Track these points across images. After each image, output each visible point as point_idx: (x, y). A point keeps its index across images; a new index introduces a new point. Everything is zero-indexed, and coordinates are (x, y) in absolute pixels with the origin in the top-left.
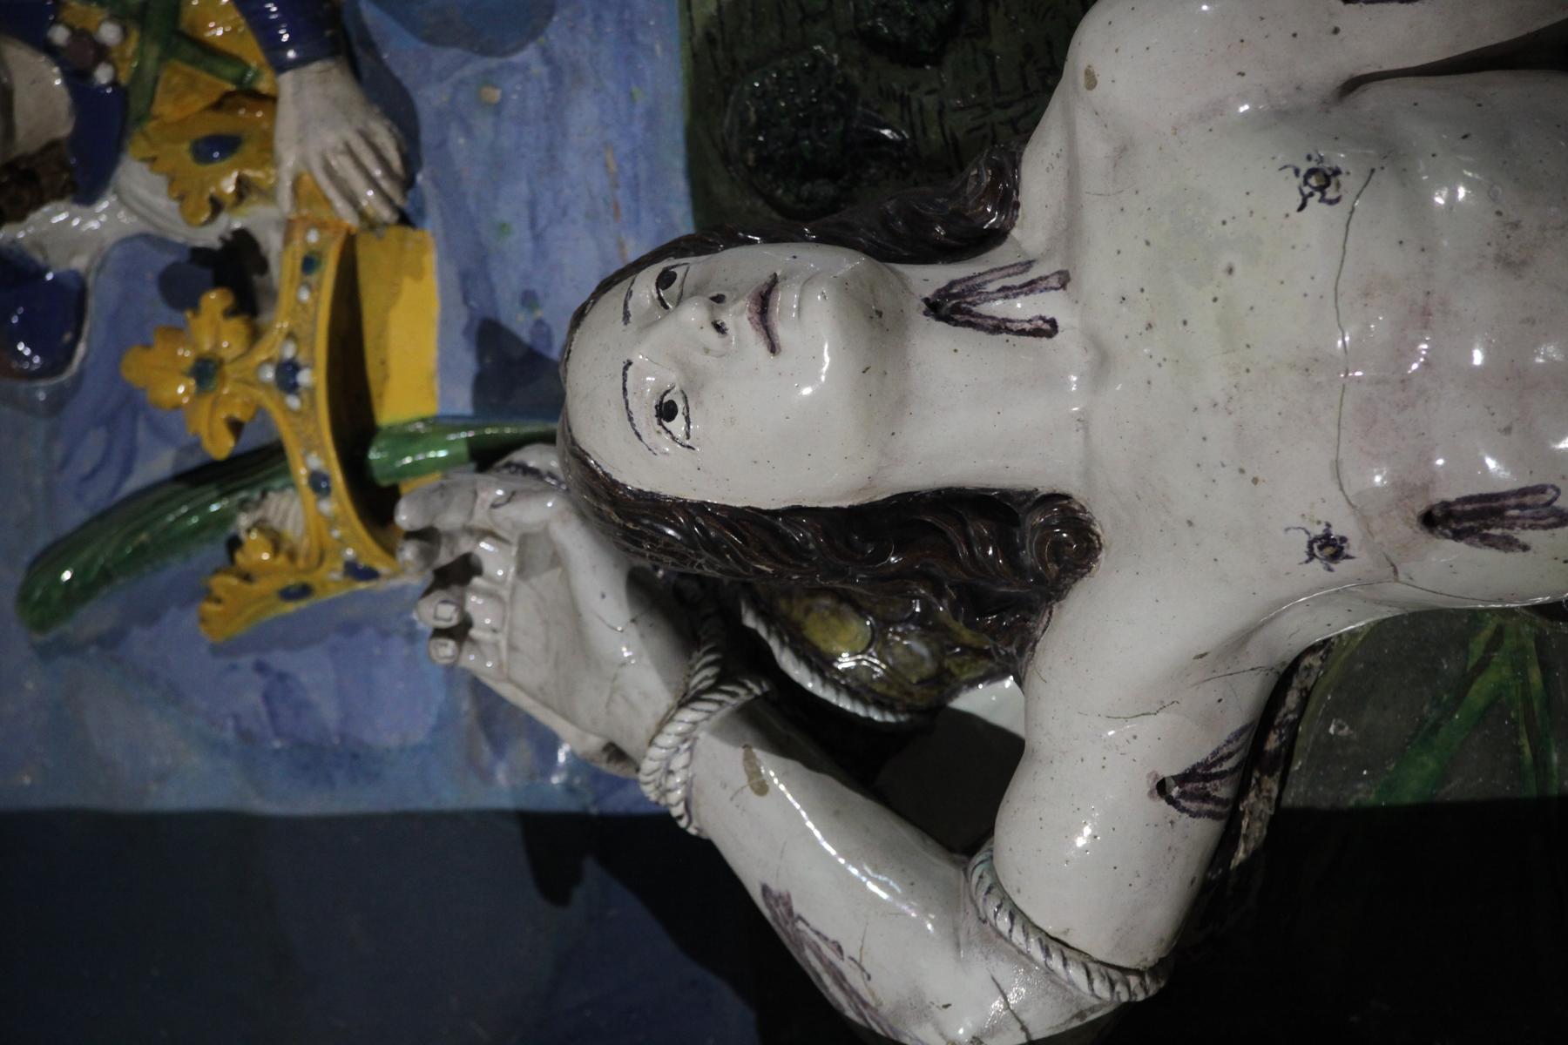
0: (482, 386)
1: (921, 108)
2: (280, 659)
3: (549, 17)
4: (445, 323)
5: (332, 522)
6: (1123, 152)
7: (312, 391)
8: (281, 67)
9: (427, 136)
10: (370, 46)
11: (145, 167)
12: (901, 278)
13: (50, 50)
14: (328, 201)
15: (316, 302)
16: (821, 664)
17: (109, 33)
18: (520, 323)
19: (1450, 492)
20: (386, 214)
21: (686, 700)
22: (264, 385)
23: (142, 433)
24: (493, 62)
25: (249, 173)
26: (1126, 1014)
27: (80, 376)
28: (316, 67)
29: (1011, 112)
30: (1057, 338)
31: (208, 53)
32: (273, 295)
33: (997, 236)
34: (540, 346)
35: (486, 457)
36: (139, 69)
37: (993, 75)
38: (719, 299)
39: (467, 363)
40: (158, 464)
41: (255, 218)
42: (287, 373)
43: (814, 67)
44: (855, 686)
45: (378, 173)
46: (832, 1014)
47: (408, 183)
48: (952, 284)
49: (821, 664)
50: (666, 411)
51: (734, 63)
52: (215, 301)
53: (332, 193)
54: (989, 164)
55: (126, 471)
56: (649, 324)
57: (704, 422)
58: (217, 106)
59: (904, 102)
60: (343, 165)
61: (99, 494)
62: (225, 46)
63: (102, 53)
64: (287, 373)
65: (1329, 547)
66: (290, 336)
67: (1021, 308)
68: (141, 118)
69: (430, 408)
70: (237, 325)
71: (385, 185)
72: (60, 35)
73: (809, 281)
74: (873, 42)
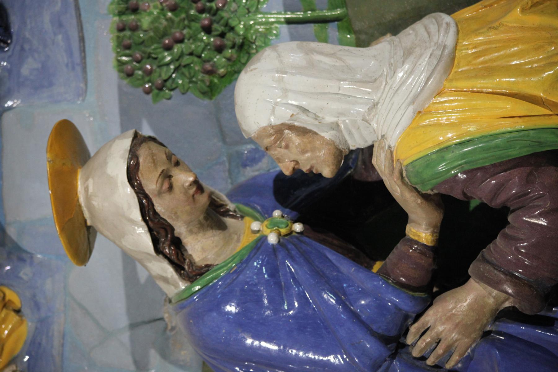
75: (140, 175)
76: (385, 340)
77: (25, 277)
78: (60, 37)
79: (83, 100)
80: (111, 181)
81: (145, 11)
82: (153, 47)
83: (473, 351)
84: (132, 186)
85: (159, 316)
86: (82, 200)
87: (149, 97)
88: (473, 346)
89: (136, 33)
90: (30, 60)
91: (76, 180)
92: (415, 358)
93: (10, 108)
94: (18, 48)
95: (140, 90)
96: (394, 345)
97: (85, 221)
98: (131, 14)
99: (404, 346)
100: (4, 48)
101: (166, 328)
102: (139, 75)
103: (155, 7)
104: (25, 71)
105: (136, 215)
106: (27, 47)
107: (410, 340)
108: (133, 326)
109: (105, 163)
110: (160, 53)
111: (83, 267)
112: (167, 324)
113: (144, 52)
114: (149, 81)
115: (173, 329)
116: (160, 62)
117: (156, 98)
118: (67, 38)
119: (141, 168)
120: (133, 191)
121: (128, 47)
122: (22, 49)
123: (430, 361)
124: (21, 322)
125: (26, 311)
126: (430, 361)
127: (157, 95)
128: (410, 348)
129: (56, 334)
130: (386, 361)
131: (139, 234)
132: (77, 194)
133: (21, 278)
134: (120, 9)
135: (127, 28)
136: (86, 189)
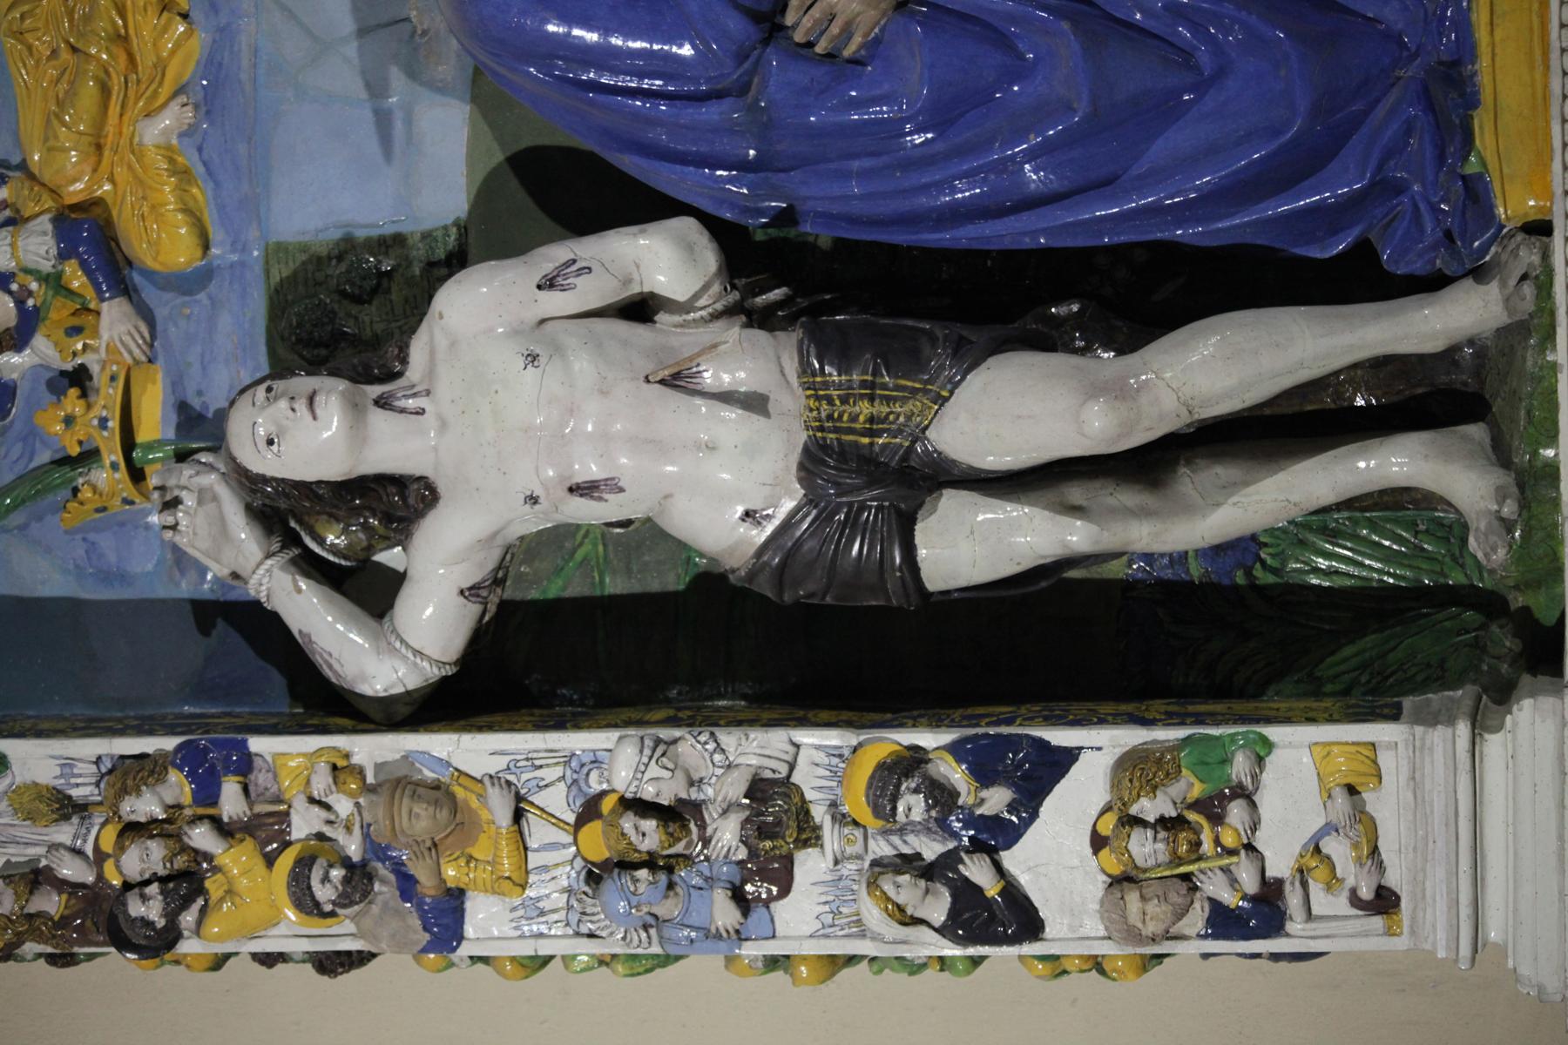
0: (180, 427)
1: (363, 322)
2: (92, 536)
3: (211, 281)
4: (164, 403)
5: (119, 482)
6: (453, 344)
7: (113, 429)
8: (103, 300)
9: (159, 328)
10: (136, 290)
11: (45, 339)
12: (364, 392)
13: (10, 293)
14: (121, 354)
15: (116, 393)
16: (321, 541)
17: (34, 286)
18: (196, 403)
19: (579, 479)
20: (143, 358)
21: (268, 556)
22: (93, 427)
23: (38, 445)
24: (187, 298)
25: (88, 341)
26: (444, 680)
27: (12, 422)
28: (117, 300)
29: (399, 324)
30: (425, 415)
31: (71, 293)
32: (97, 391)
33: (400, 375)
34: (204, 412)
35: (182, 457)
36: (45, 300)
37: (392, 309)
38: (293, 398)
39: (173, 418)
40: (44, 457)
41: (92, 361)
42: (103, 422)
43: (319, 304)
44: (333, 549)
45: (140, 342)
46: (326, 682)
47: (151, 346)
48: (383, 393)
49: (321, 541)
50: (270, 442)
51: (286, 301)
52: (73, 392)
53: (123, 350)
54: (397, 346)
55: (31, 460)
56: (263, 408)
57: (285, 446)
58: (73, 314)
59: (356, 318)
60: (127, 339)
61: (19, 469)
62: (79, 291)
63: (30, 294)
64: (103, 422)
65: (533, 500)
66: (104, 407)
67: (411, 403)
68: (44, 319)
69: (157, 436)
70: (82, 402)
71: (144, 347)
72: (14, 287)
73: (329, 392)
74: (343, 294)
76: (756, 17)
83: (882, 30)
88: (882, 22)
92: (798, 45)
96: (768, 25)
99: (782, 28)
101: (414, 32)
107: (789, 19)
108: (363, 32)
115: (425, 33)
123: (819, 49)
124: (189, 33)
126: (819, 49)
128: (790, 32)
130: (755, 49)
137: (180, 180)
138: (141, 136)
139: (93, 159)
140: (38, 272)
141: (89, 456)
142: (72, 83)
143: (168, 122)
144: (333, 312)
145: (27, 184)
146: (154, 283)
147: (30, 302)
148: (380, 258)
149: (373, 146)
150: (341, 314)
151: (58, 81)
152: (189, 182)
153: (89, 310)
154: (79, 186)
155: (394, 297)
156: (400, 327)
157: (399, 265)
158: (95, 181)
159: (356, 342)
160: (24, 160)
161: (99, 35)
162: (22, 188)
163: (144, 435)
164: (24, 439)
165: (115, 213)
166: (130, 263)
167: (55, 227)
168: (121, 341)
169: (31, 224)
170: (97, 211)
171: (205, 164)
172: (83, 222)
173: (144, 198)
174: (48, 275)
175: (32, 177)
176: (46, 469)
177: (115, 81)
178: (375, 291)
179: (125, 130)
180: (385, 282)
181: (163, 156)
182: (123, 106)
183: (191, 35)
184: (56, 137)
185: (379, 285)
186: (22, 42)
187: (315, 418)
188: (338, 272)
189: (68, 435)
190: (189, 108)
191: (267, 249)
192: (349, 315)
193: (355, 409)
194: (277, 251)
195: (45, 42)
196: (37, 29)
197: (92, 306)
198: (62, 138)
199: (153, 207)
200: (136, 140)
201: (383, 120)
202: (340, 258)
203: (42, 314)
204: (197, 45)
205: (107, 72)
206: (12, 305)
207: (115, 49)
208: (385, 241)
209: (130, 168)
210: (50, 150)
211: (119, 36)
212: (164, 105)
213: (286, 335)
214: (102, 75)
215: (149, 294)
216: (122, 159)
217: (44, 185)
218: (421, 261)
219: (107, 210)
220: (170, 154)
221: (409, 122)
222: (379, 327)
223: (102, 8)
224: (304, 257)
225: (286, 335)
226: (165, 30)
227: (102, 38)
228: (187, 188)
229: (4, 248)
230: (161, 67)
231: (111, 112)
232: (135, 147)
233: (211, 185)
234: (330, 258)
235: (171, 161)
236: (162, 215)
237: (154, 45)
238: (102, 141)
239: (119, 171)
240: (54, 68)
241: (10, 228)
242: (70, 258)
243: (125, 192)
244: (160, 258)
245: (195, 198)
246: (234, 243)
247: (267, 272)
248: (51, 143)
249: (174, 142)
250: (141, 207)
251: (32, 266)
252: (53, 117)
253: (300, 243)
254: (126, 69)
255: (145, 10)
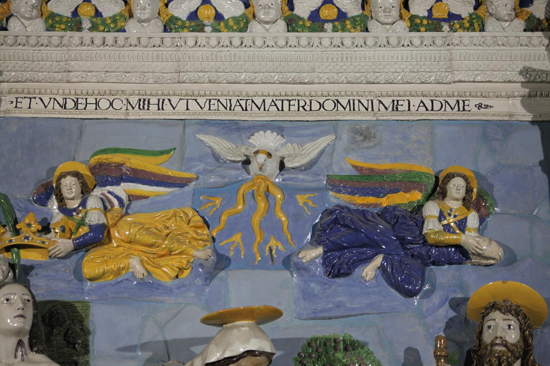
4: (34, 261)
5: (5, 242)
7: (24, 241)
8: (73, 240)
10: (77, 253)
12: (27, 335)
13: (79, 206)
14: (52, 246)
15: (37, 243)
18: (33, 272)
20: (50, 254)
22: (26, 234)
23: (23, 213)
27: (32, 204)
28: (73, 246)
29: (55, 350)
30: (14, 359)
31: (78, 229)
32: (40, 236)
33: (32, 350)
34: (29, 275)
38: (23, 309)
40: (18, 215)
41: (51, 235)
42: (27, 238)
43: (65, 321)
45: (56, 253)
47: (55, 257)
48: (24, 343)
50: (7, 300)
51: (68, 308)
52: (40, 228)
53: (53, 247)
54: (42, 349)
55: (18, 210)
56: (21, 299)
58: (70, 229)
59: (59, 334)
60: (58, 249)
61: (15, 206)
63: (78, 214)
64: (27, 238)
66: (33, 239)
68: (68, 218)
69: (22, 257)
70: (36, 230)
71: (54, 254)
72: (80, 208)
73: (24, 323)
74: (68, 330)
75: (250, 357)
77: (196, 281)
78: (332, 306)
79: (295, 317)
80: (247, 341)
81: (345, 355)
82: (324, 359)
84: (244, 353)
85: (171, 358)
86: (237, 323)
87: (296, 355)
89: (333, 349)
90: (319, 288)
91: (249, 320)
93: (292, 275)
94: (326, 281)
95: (301, 351)
97: (226, 324)
98: (343, 347)
100: (326, 273)
101: (164, 362)
102: (309, 351)
103: (347, 361)
104: (313, 285)
105: (227, 355)
106: (327, 286)
108: (166, 342)
109: (257, 337)
110: (321, 363)
111: (200, 321)
112: (166, 362)
113: (322, 353)
114: (305, 356)
116: (316, 362)
117: (295, 360)
118: (330, 310)
119: (254, 358)
120: (241, 353)
121: (325, 344)
122: (325, 284)
124: (171, 278)
125: (177, 281)
127: (297, 360)
129: (164, 298)
131: (216, 355)
132: (241, 320)
133: (196, 279)
134: (346, 341)
135: (336, 344)
136: (243, 326)
137: (115, 272)
138: (133, 258)
139: (126, 240)
140: (86, 217)
141: (17, 232)
142: (155, 234)
143: (138, 269)
144: (62, 326)
145: (119, 215)
146: (80, 258)
147: (74, 214)
148: (81, 345)
149: (122, 344)
150: (61, 329)
151: (156, 229)
152: (115, 275)
153: (71, 235)
154: (117, 235)
155: (66, 349)
156: (54, 351)
157: (77, 351)
158: (118, 240)
159: (49, 334)
160: (129, 214)
161: (172, 245)
162: (117, 213)
163: (23, 253)
164: (26, 208)
165: (106, 247)
166: (87, 251)
167: (101, 224)
168: (57, 246)
169: (103, 216)
170: (107, 240)
171: (121, 281)
172: (103, 236)
173: (110, 258)
174: (84, 221)
175: (122, 217)
176: (14, 215)
177: (154, 250)
178: (68, 342)
179: (136, 252)
180: (71, 346)
181: (125, 266)
182: (145, 252)
183: (171, 279)
184: (134, 227)
185: (71, 344)
186: (172, 216)
187: (15, 317)
188: (77, 328)
189: (25, 225)
190: (142, 276)
191: (88, 302)
192: (60, 332)
193: (18, 332)
194: (86, 306)
195: (171, 224)
196: (176, 222)
197: (73, 236)
198: (134, 229)
199: (106, 261)
200: (133, 256)
201: (132, 348)
202: (82, 329)
203: (70, 218)
204: (166, 281)
205: (158, 247)
206: (75, 207)
207: (166, 250)
208: (87, 347)
209: (123, 253)
210: (130, 224)
211: (171, 252)
212: (144, 267)
213: (55, 308)
214: (157, 245)
215: (75, 258)
216: (125, 250)
217: (118, 221)
218: (78, 360)
219: (107, 244)
220: (126, 268)
221: (131, 358)
222: (54, 343)
223: (182, 246)
224: (84, 316)
225: (55, 308)
226: (172, 269)
227: (170, 245)
228: (113, 274)
229: (95, 205)
230: (159, 267)
231: (143, 247)
232: (129, 256)
233: (114, 283)
234: (82, 326)
235: (123, 269)
236: (103, 264)
237: (167, 265)
238: (133, 244)
239: (122, 248)
240: (161, 227)
241: (102, 208)
242: (90, 229)
243: (114, 251)
244: (87, 262)
245: (108, 277)
246: (91, 290)
247: (79, 302)
248: (133, 225)
249: (131, 270)
250: (107, 256)
251: (88, 215)
252: (142, 226)
253: (89, 315)
254: (159, 254)
255: (180, 262)
